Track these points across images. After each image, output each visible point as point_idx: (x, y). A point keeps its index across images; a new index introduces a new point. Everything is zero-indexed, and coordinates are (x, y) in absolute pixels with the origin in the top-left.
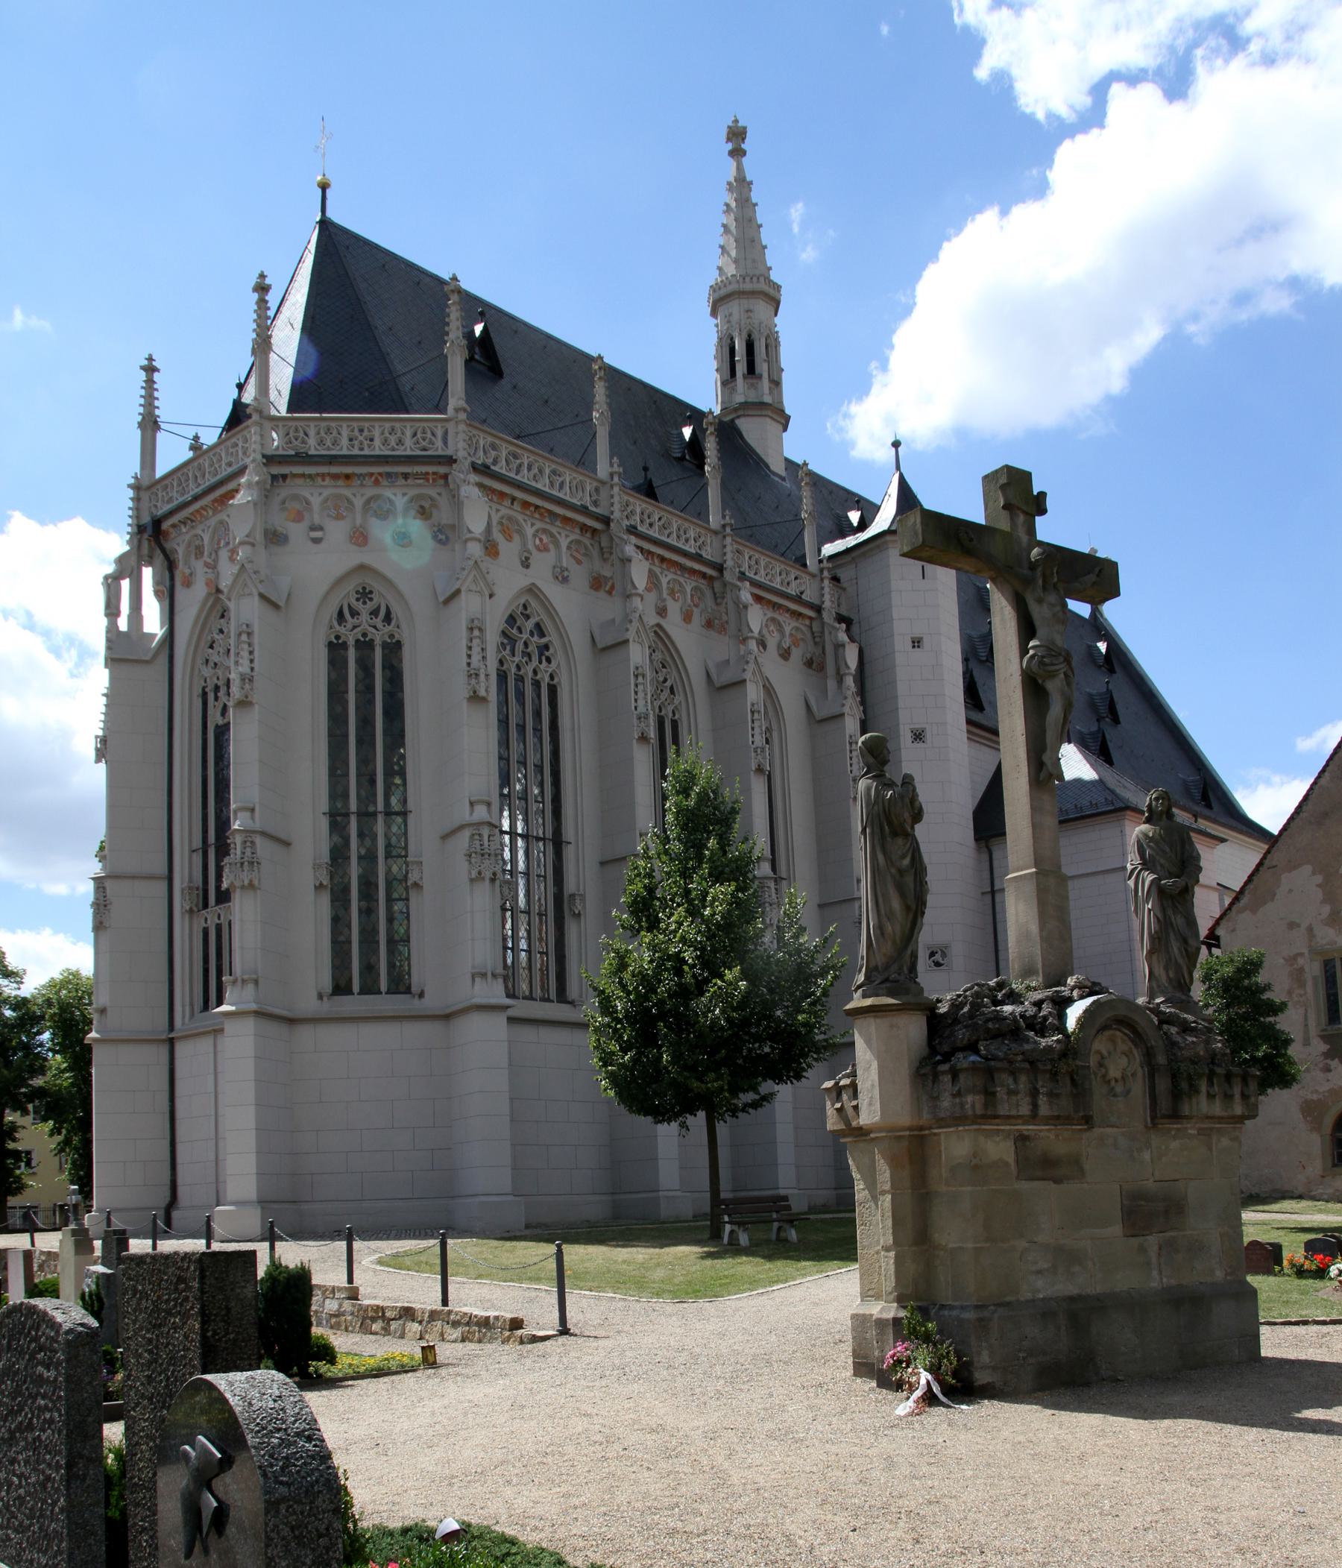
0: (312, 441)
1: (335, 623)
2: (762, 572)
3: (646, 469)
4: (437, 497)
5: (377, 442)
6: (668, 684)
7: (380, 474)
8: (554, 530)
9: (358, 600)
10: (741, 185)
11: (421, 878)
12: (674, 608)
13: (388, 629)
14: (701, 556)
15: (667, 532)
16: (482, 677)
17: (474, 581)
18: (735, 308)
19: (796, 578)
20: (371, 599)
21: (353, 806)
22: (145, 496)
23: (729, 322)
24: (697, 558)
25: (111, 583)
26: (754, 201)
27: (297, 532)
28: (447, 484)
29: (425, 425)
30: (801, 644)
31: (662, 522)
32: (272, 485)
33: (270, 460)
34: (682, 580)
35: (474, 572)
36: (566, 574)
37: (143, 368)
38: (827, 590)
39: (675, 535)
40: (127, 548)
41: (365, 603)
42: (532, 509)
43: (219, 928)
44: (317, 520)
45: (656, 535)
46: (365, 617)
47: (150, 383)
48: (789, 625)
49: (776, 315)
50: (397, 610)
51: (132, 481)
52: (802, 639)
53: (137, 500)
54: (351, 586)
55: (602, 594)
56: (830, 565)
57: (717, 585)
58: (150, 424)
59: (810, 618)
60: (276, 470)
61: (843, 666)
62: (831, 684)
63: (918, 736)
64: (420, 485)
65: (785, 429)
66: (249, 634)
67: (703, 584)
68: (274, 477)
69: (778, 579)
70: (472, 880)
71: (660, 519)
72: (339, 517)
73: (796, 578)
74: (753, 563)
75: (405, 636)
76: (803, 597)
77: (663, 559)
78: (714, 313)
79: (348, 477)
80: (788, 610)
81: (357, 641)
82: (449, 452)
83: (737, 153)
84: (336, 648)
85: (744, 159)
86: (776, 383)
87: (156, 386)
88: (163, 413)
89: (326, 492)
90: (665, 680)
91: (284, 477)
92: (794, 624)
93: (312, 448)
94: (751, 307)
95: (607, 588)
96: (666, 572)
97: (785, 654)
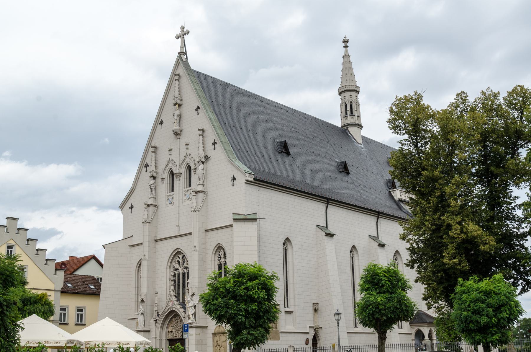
10: (346, 56)
26: (351, 61)
86: (359, 117)
94: (351, 94)
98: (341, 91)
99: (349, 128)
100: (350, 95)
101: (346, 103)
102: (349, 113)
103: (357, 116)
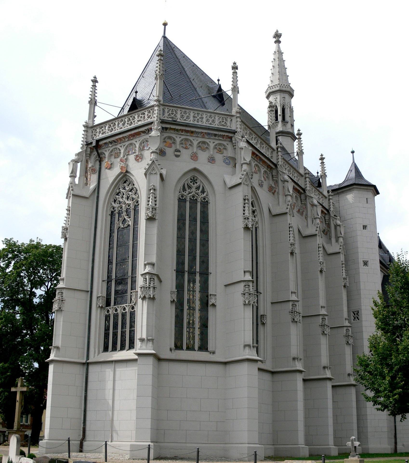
0: (179, 116)
4: (226, 145)
5: (204, 120)
7: (206, 133)
8: (260, 165)
9: (191, 182)
10: (279, 53)
11: (216, 302)
20: (196, 183)
21: (186, 268)
22: (90, 131)
23: (276, 100)
27: (170, 151)
28: (231, 141)
29: (223, 116)
35: (246, 177)
40: (81, 150)
41: (194, 184)
42: (255, 156)
43: (124, 315)
44: (178, 147)
46: (194, 190)
47: (94, 86)
50: (207, 188)
51: (85, 124)
54: (189, 176)
55: (271, 194)
56: (333, 194)
57: (303, 196)
58: (93, 103)
59: (325, 214)
61: (339, 233)
62: (333, 240)
64: (220, 140)
66: (154, 190)
70: (245, 305)
72: (186, 148)
75: (211, 199)
78: (268, 97)
79: (192, 132)
81: (190, 199)
82: (233, 128)
83: (278, 42)
84: (181, 201)
85: (280, 44)
88: (98, 99)
89: (183, 137)
91: (166, 129)
93: (179, 119)
95: (273, 191)
102: (280, 118)
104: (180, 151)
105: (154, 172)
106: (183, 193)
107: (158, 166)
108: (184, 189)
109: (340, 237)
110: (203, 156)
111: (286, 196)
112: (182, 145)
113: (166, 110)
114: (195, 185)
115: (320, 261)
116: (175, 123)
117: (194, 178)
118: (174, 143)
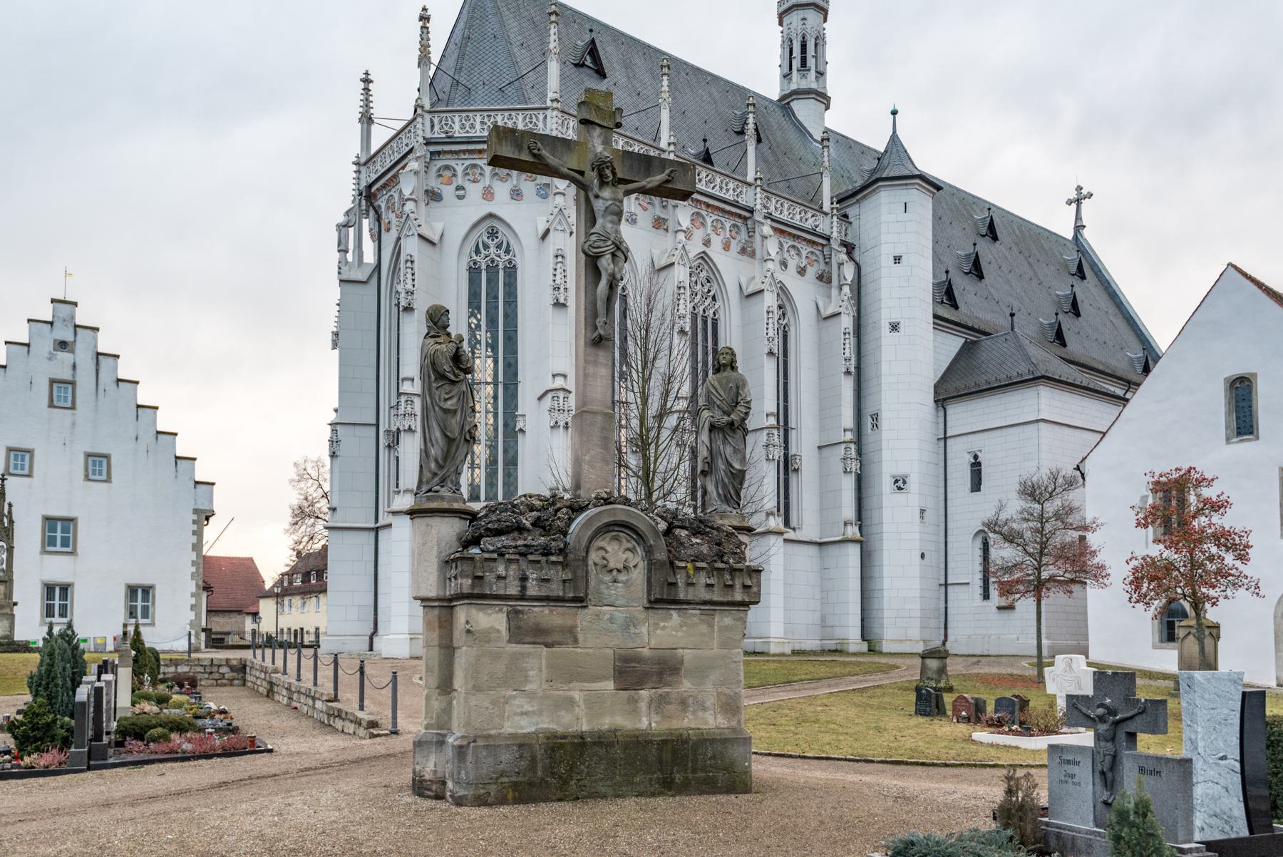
0: (457, 127)
1: (474, 254)
2: (786, 213)
3: (705, 140)
6: (711, 294)
9: (488, 238)
12: (717, 242)
13: (508, 257)
14: (738, 202)
15: (712, 185)
16: (562, 290)
17: (560, 223)
18: (795, 18)
19: (813, 216)
20: (497, 237)
24: (735, 204)
25: (343, 227)
27: (448, 191)
29: (532, 112)
30: (815, 264)
31: (709, 178)
32: (431, 159)
33: (428, 143)
34: (723, 219)
35: (560, 217)
36: (634, 217)
37: (362, 80)
38: (835, 224)
39: (718, 188)
41: (493, 240)
45: (704, 188)
46: (493, 250)
48: (805, 249)
49: (825, 21)
52: (816, 260)
53: (358, 172)
54: (483, 228)
55: (661, 231)
56: (838, 206)
57: (749, 222)
59: (823, 246)
60: (433, 148)
62: (834, 292)
63: (895, 327)
65: (827, 108)
66: (412, 262)
67: (739, 222)
68: (432, 153)
69: (798, 217)
71: (707, 176)
73: (813, 216)
74: (778, 206)
76: (817, 229)
77: (708, 205)
80: (805, 239)
84: (474, 272)
86: (820, 74)
87: (370, 93)
89: (467, 163)
90: (709, 291)
91: (439, 153)
92: (810, 249)
94: (806, 16)
96: (711, 215)
97: (802, 271)
98: (782, 9)
99: (795, 102)
100: (802, 16)
101: (791, 41)
103: (817, 72)
104: (464, 189)
105: (411, 233)
106: (475, 257)
107: (414, 222)
108: (477, 252)
109: (843, 285)
110: (502, 190)
111: (676, 232)
112: (468, 177)
113: (436, 121)
114: (496, 240)
115: (769, 335)
116: (450, 140)
117: (493, 230)
118: (455, 175)
